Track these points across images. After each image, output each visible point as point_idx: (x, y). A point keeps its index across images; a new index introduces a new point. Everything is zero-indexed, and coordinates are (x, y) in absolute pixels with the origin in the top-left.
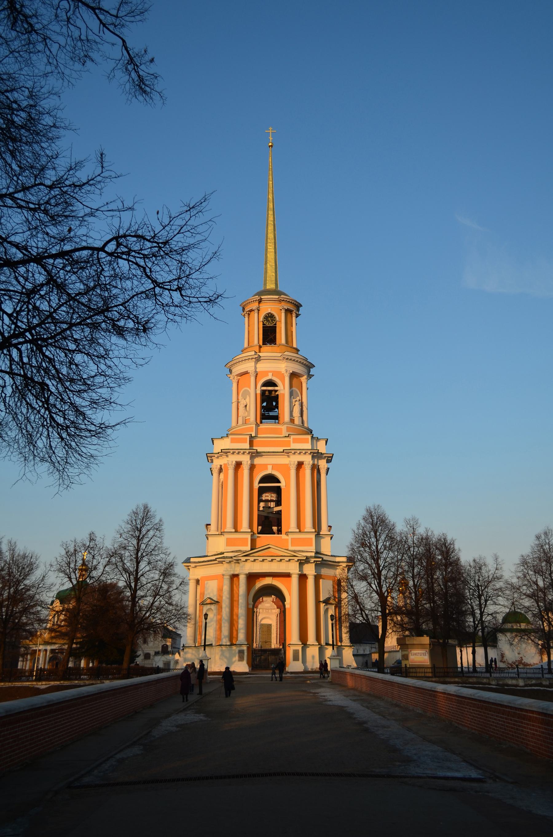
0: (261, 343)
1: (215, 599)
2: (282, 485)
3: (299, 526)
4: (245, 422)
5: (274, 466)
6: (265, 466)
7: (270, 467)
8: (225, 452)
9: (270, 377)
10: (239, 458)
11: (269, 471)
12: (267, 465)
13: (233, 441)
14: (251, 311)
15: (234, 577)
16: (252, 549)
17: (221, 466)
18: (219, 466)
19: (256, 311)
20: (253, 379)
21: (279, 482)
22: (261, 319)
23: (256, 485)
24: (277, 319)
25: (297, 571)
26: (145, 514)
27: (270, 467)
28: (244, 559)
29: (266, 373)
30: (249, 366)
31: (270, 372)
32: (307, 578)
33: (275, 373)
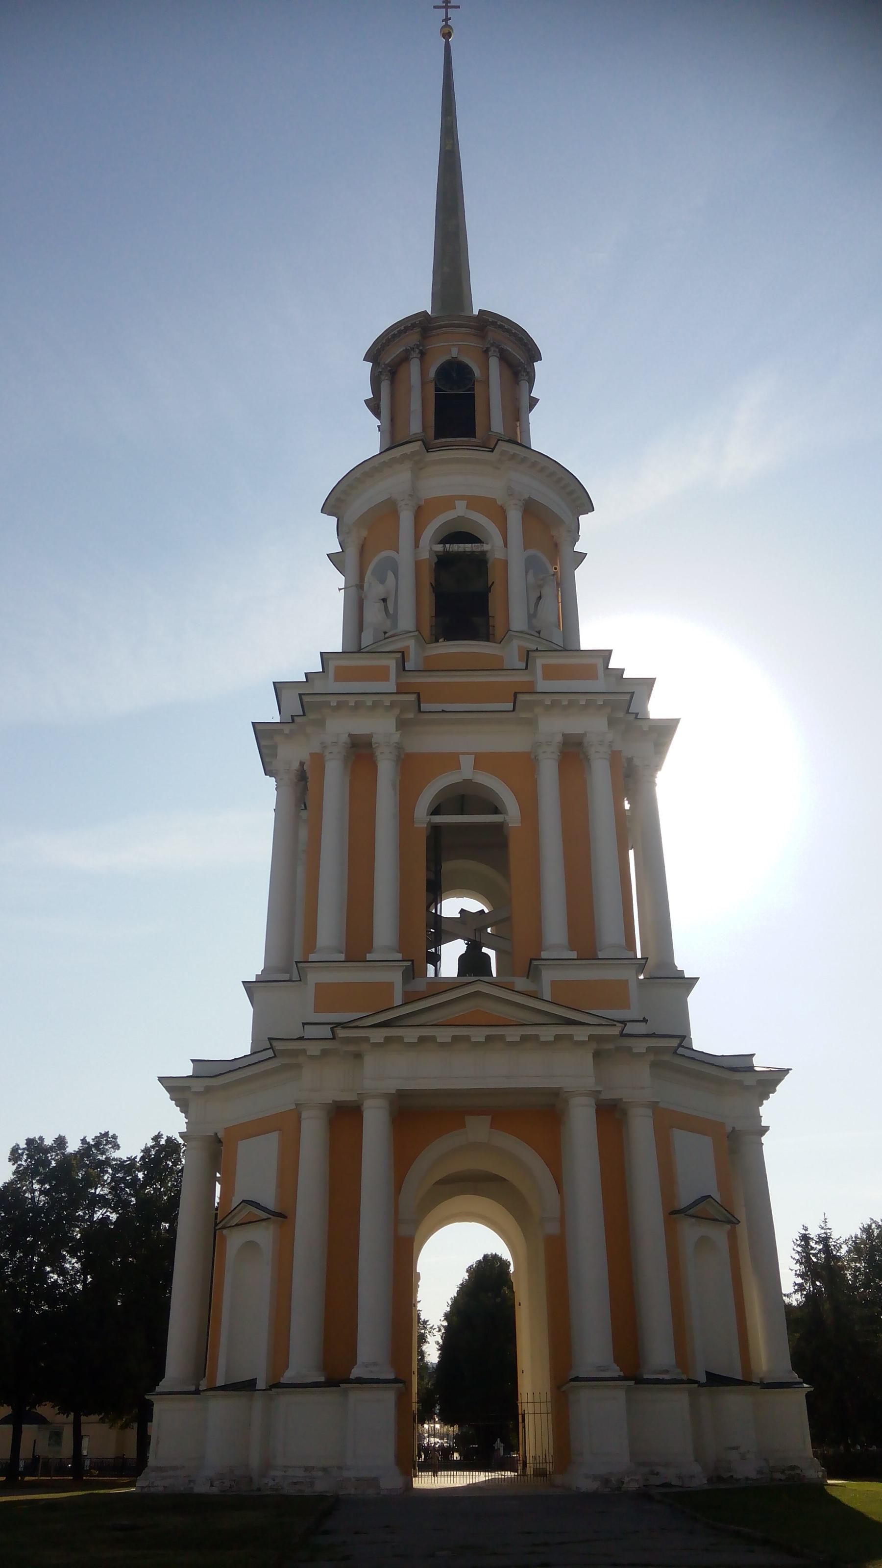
0: (431, 432)
1: (270, 1202)
5: (482, 761)
6: (451, 761)
10: (361, 725)
11: (467, 771)
14: (404, 359)
15: (344, 1117)
16: (404, 1004)
17: (302, 764)
18: (296, 765)
19: (415, 354)
20: (406, 518)
22: (432, 373)
24: (477, 373)
25: (589, 1082)
26: (161, 1079)
28: (377, 1036)
29: (448, 502)
31: (462, 498)
32: (624, 1113)
33: (473, 502)
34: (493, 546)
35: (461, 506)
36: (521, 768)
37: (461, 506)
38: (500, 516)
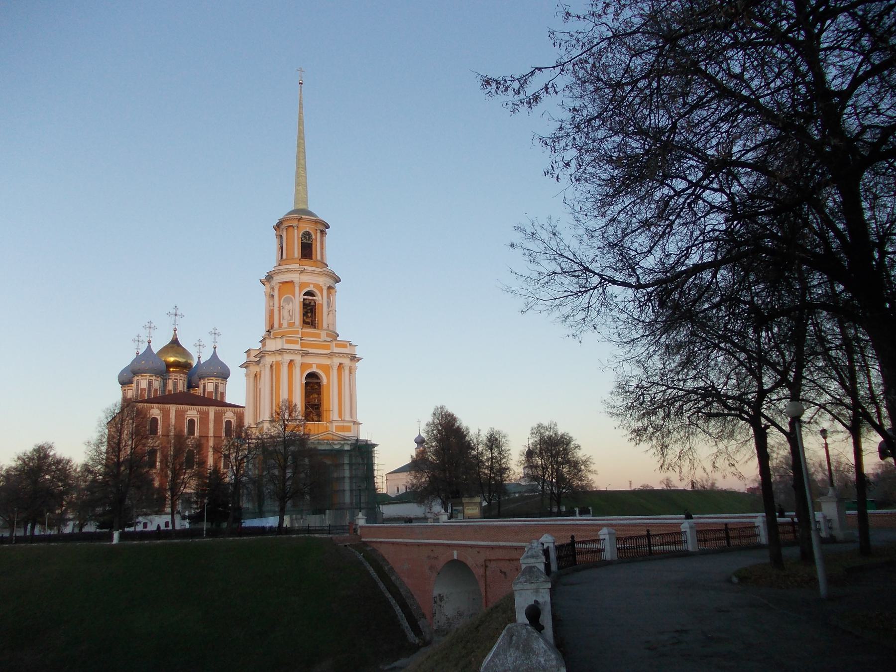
2: (324, 380)
3: (340, 415)
4: (291, 325)
5: (319, 366)
7: (314, 366)
8: (281, 352)
9: (311, 288)
11: (314, 369)
12: (315, 364)
13: (288, 342)
20: (297, 289)
21: (319, 378)
23: (304, 381)
24: (314, 237)
27: (314, 366)
29: (308, 284)
30: (295, 277)
33: (317, 286)
34: (318, 298)
35: (312, 286)
36: (327, 368)
37: (312, 286)
38: (321, 291)
